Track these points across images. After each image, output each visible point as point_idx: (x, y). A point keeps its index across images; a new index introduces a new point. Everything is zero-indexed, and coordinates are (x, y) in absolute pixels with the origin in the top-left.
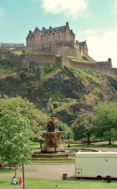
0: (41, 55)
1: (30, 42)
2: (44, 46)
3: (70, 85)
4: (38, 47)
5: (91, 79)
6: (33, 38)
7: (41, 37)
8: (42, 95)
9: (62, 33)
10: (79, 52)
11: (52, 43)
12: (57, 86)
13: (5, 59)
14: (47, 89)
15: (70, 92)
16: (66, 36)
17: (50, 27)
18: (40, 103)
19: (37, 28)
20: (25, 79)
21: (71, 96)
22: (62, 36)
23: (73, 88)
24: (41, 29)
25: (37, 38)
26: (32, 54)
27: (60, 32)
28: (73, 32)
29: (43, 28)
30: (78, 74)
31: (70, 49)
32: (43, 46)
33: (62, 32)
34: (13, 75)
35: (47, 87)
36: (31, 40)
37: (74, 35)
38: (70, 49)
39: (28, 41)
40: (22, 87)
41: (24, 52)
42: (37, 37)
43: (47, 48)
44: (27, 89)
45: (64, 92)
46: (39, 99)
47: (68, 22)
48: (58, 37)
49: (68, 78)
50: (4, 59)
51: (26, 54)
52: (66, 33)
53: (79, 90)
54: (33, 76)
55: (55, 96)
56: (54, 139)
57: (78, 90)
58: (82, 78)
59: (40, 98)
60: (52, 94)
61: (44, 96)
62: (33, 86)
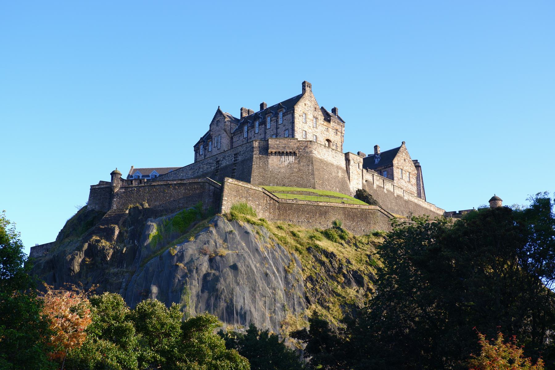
1: (203, 156)
2: (220, 162)
4: (205, 167)
5: (331, 256)
7: (232, 138)
9: (284, 118)
10: (340, 174)
11: (240, 149)
17: (262, 105)
19: (219, 112)
25: (217, 143)
26: (138, 184)
27: (281, 115)
29: (241, 109)
33: (284, 115)
36: (206, 151)
38: (296, 165)
39: (198, 155)
43: (226, 167)
47: (308, 81)
48: (275, 131)
50: (93, 210)
52: (296, 115)
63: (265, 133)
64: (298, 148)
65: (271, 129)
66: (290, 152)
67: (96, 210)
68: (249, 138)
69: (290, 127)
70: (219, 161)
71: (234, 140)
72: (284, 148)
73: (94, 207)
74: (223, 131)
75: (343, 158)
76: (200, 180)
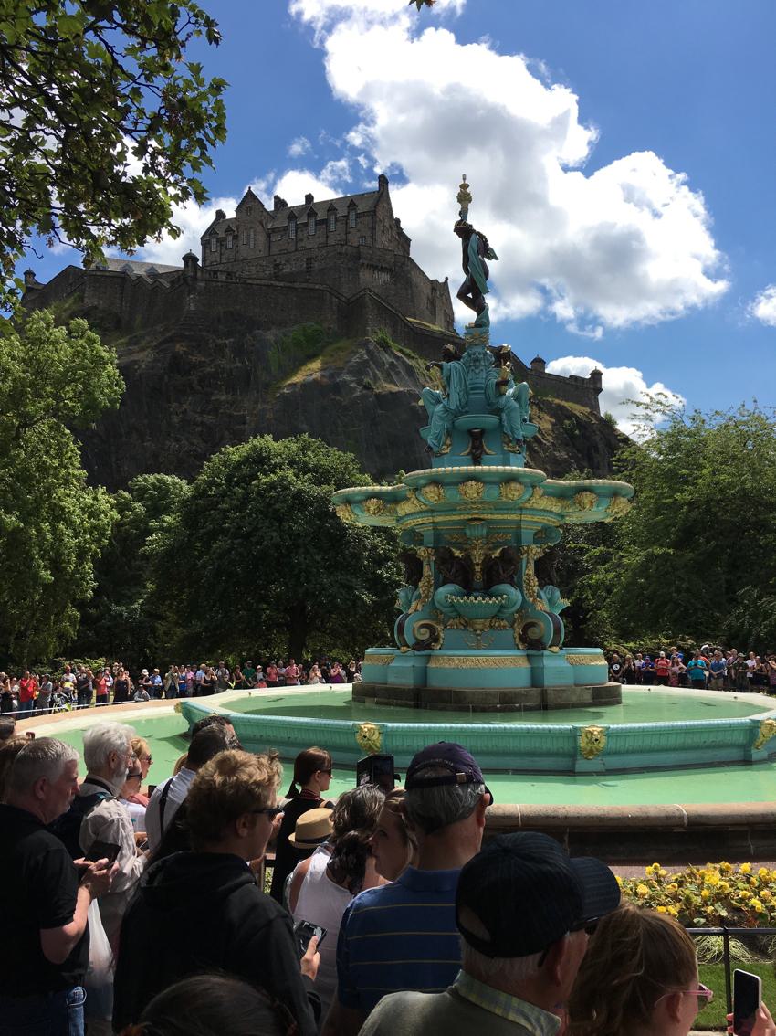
0: (272, 285)
2: (281, 267)
6: (230, 238)
7: (269, 236)
9: (358, 220)
13: (102, 304)
16: (378, 233)
17: (309, 198)
22: (358, 234)
24: (270, 206)
25: (249, 238)
27: (352, 215)
28: (402, 225)
31: (395, 285)
32: (277, 266)
33: (358, 216)
34: (135, 362)
37: (408, 241)
38: (393, 286)
39: (208, 251)
40: (176, 420)
41: (190, 264)
42: (252, 234)
44: (199, 429)
48: (344, 237)
50: (96, 308)
51: (199, 274)
54: (231, 370)
62: (230, 416)
63: (327, 237)
64: (395, 263)
65: (337, 232)
66: (386, 268)
67: (100, 307)
68: (298, 239)
69: (369, 233)
70: (278, 265)
71: (273, 239)
72: (379, 260)
73: (96, 303)
74: (258, 224)
75: (430, 286)
76: (317, 287)
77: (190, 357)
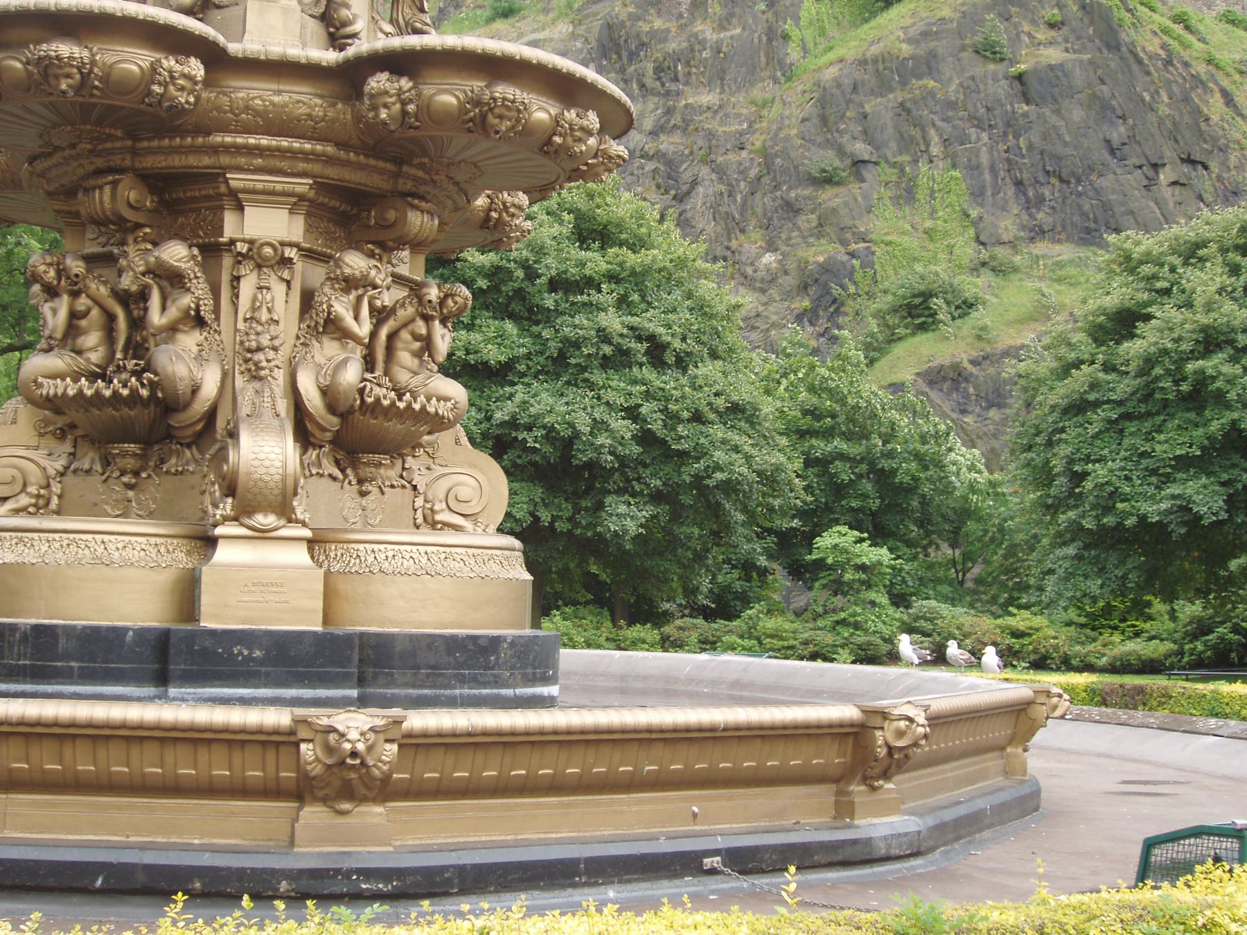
3: (1077, 114)
8: (791, 209)
12: (939, 123)
14: (841, 152)
15: (1079, 181)
18: (763, 291)
20: (640, 77)
21: (1088, 231)
23: (1112, 151)
30: (1166, 31)
35: (845, 139)
45: (1011, 191)
46: (760, 256)
49: (1054, 55)
53: (1164, 177)
55: (917, 219)
56: (173, 279)
57: (1155, 167)
58: (1201, 69)
59: (771, 247)
60: (896, 200)
61: (807, 221)
77: (640, 23)
